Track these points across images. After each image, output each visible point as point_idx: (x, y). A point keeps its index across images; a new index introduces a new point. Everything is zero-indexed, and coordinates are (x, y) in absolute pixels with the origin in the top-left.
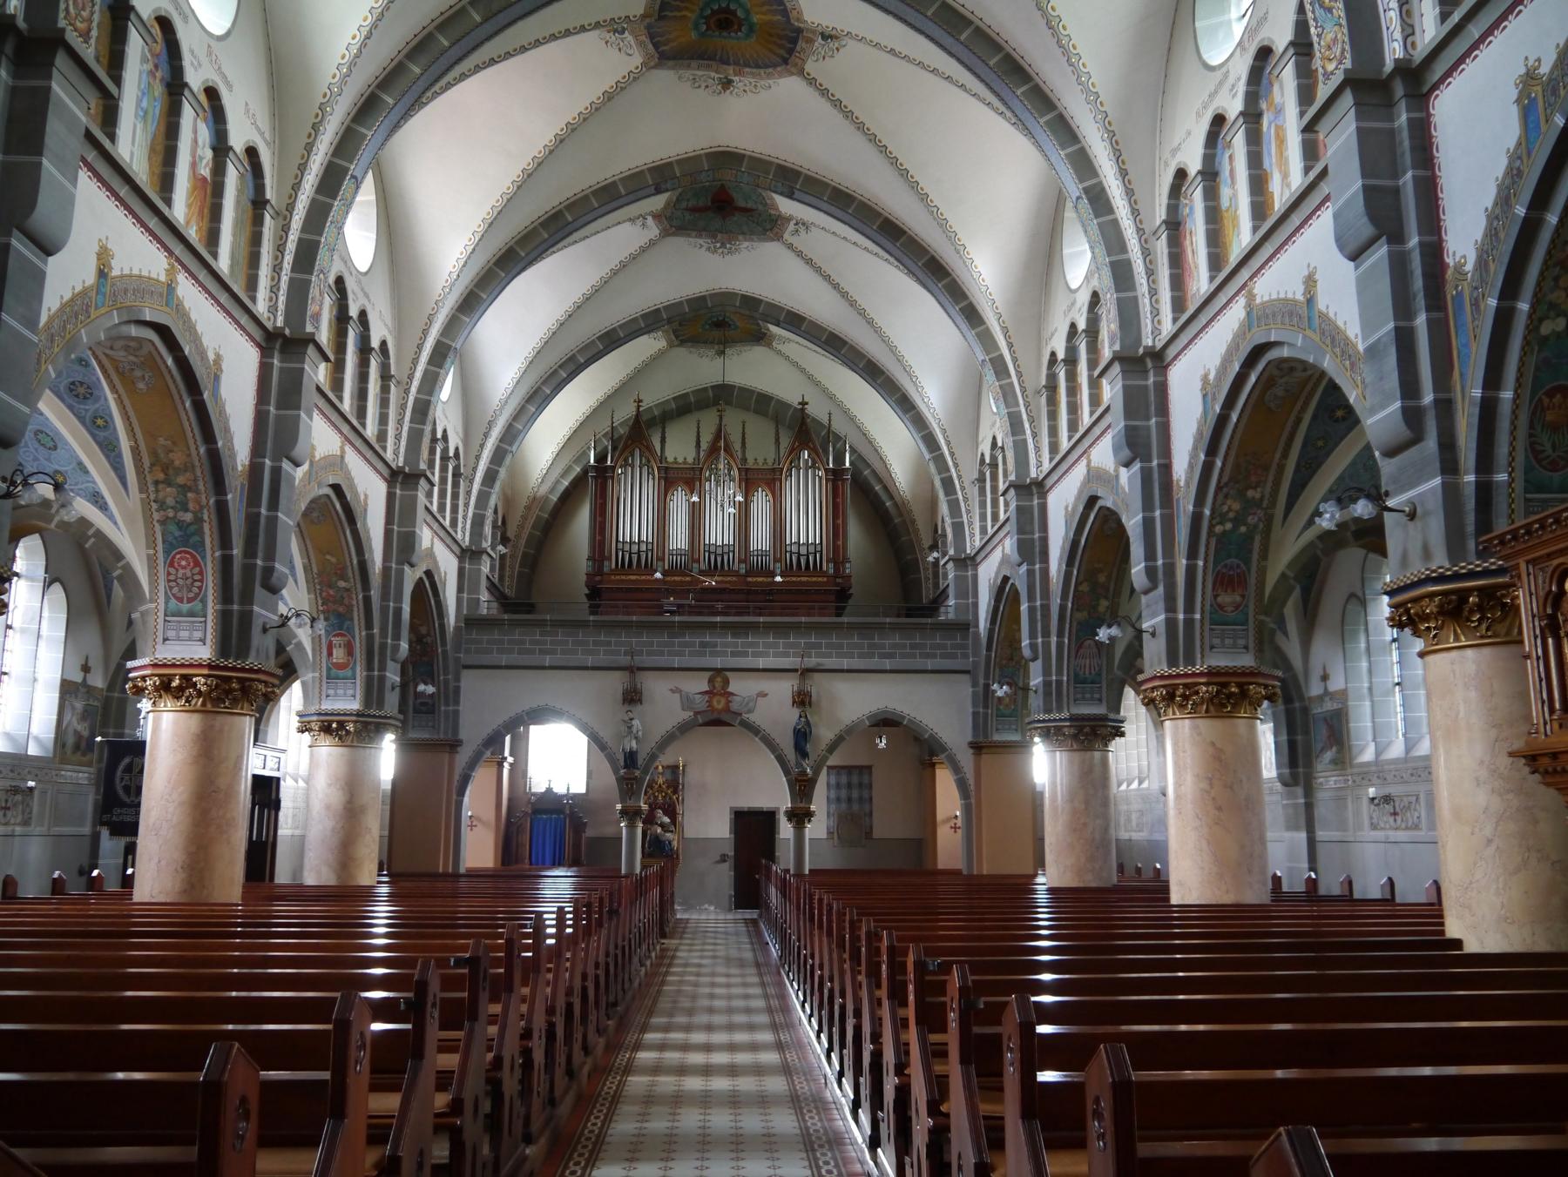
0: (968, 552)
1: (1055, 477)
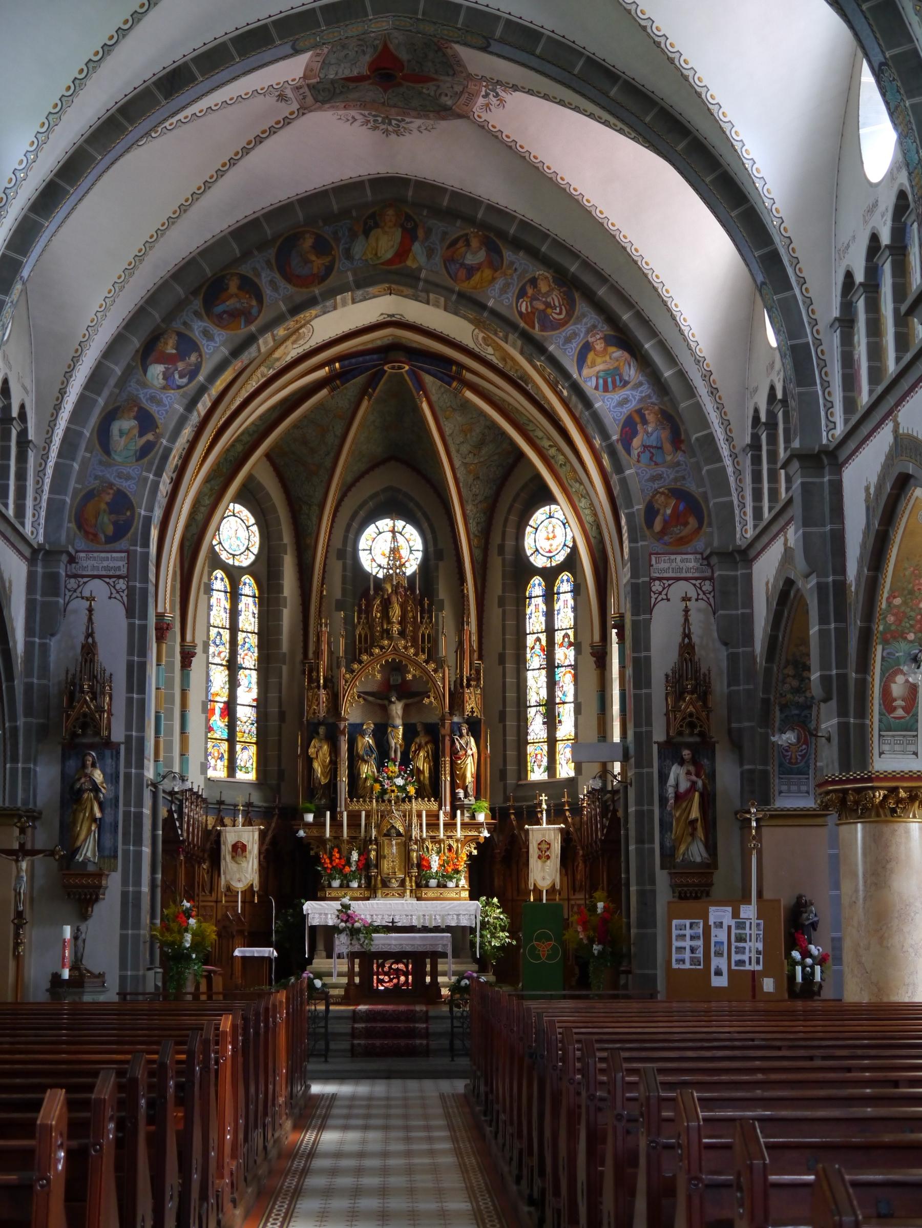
0: (738, 542)
1: (852, 445)
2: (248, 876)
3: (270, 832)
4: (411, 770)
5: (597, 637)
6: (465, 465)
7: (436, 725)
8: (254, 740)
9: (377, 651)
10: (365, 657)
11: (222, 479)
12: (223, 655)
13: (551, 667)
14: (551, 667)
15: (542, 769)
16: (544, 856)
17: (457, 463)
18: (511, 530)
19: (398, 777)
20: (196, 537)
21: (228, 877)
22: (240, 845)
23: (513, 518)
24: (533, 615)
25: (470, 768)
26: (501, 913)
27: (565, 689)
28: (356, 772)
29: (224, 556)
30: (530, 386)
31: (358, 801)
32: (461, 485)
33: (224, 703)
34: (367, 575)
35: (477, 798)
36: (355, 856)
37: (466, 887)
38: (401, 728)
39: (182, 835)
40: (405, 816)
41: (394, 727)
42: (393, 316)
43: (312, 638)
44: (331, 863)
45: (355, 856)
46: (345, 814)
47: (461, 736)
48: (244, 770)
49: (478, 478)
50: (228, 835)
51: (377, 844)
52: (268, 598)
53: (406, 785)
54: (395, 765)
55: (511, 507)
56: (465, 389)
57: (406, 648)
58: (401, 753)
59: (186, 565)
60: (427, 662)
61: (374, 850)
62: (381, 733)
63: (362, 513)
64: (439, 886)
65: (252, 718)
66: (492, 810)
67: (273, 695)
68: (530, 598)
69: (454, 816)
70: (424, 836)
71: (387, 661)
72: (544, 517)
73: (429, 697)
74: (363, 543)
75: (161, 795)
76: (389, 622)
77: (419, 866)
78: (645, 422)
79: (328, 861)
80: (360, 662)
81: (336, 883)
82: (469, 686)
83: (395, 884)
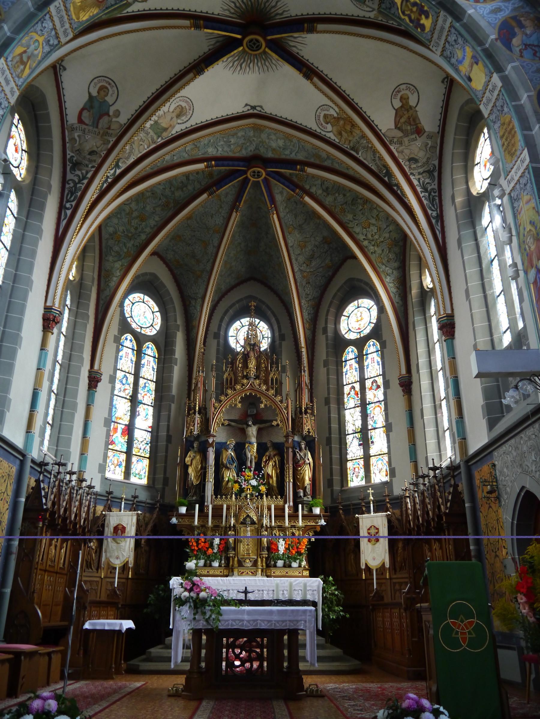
2: (125, 554)
3: (152, 521)
4: (263, 475)
5: (404, 371)
6: (301, 271)
8: (148, 456)
10: (229, 392)
11: (130, 258)
12: (127, 392)
13: (364, 405)
14: (364, 405)
15: (359, 479)
16: (374, 538)
17: (296, 269)
18: (331, 318)
20: (108, 298)
21: (108, 555)
22: (120, 527)
23: (333, 310)
24: (348, 372)
25: (307, 474)
26: (335, 590)
28: (221, 477)
29: (134, 326)
30: (360, 153)
31: (221, 498)
32: (298, 284)
33: (125, 425)
34: (232, 351)
35: (314, 496)
36: (217, 541)
37: (307, 567)
38: (255, 445)
39: (46, 504)
40: (258, 508)
41: (250, 443)
42: (254, 108)
44: (197, 546)
45: (217, 541)
47: (301, 450)
48: (138, 476)
49: (309, 283)
50: (111, 518)
51: (235, 530)
52: (164, 358)
53: (259, 485)
54: (251, 471)
55: (331, 302)
56: (304, 195)
57: (259, 385)
59: (100, 317)
62: (240, 448)
63: (231, 312)
64: (285, 566)
65: (147, 440)
67: (163, 424)
68: (346, 361)
69: (296, 510)
70: (273, 524)
71: (246, 395)
72: (354, 308)
74: (232, 332)
75: (29, 464)
77: (269, 549)
78: (521, 26)
79: (195, 544)
80: (227, 395)
82: (306, 413)
83: (248, 563)
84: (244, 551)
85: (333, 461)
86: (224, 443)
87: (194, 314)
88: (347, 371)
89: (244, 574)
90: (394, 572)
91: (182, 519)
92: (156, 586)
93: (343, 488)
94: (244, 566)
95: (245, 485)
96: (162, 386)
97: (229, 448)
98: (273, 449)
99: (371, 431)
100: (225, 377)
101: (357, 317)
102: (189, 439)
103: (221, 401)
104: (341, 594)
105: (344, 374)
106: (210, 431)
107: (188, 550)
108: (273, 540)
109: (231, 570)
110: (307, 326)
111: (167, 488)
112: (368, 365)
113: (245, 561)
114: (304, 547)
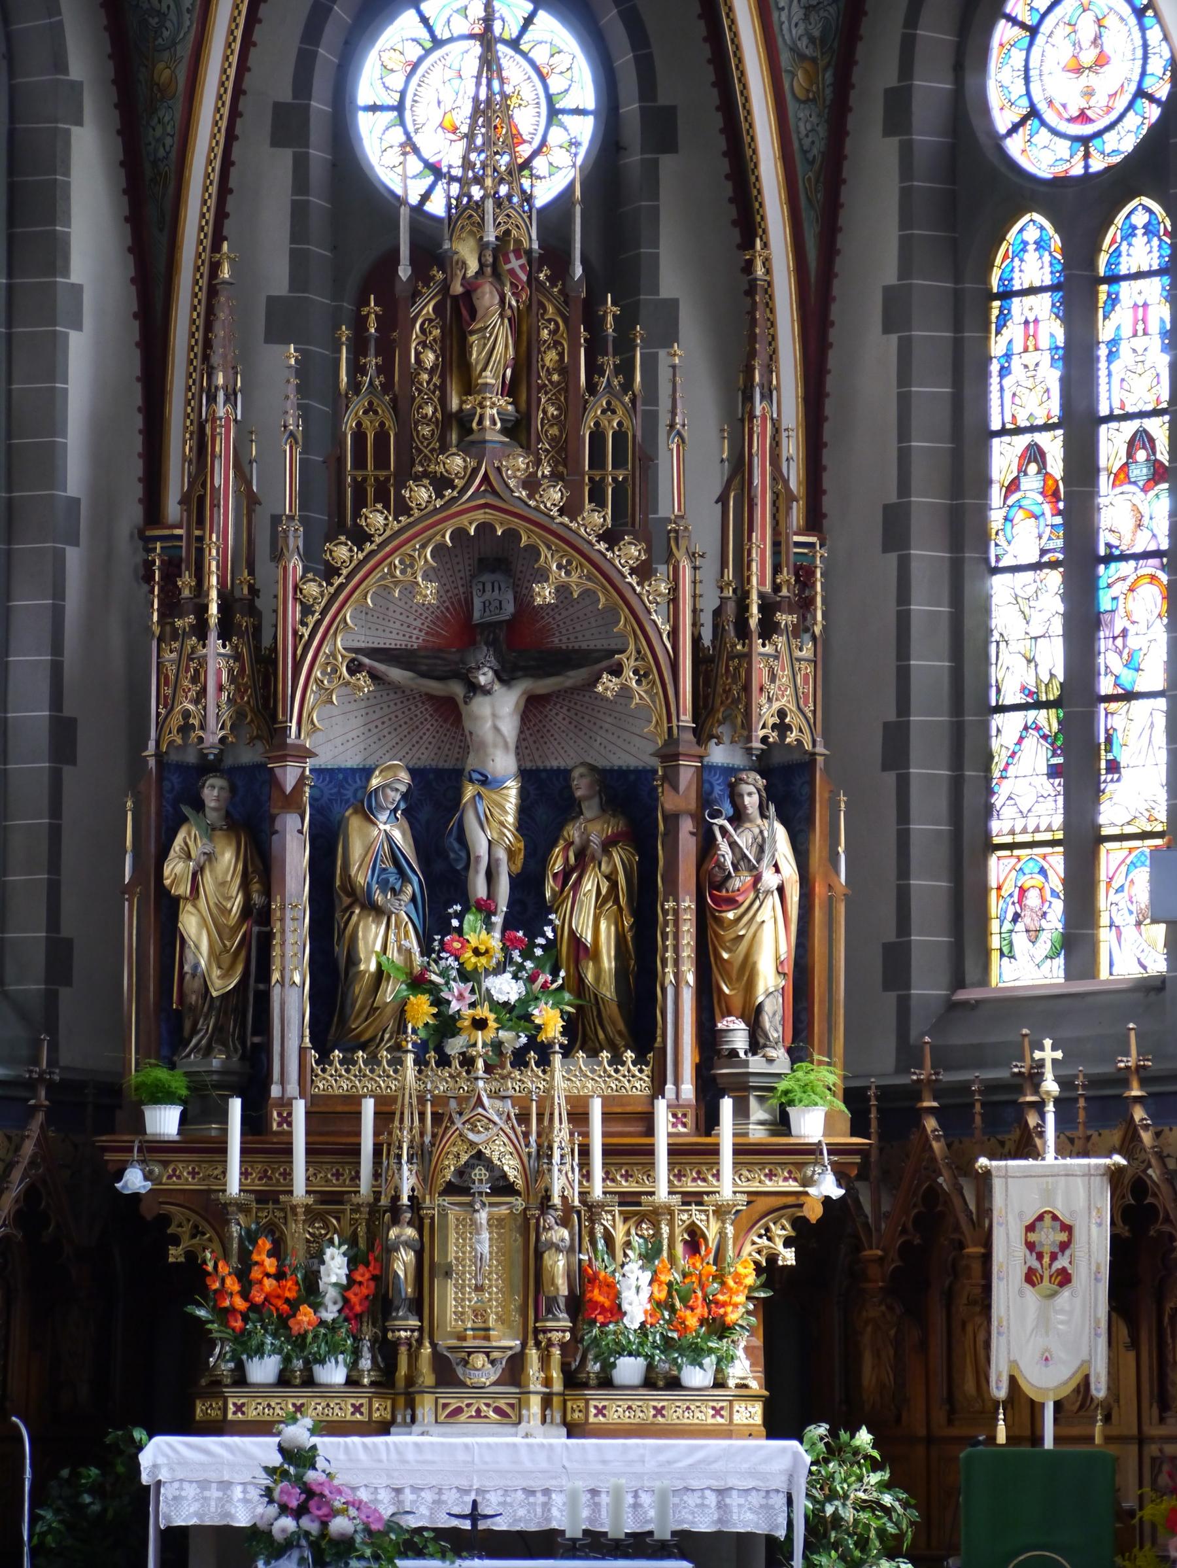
3: (16, 1174)
4: (550, 946)
7: (644, 775)
9: (422, 494)
10: (376, 519)
15: (1044, 945)
19: (499, 970)
24: (1016, 363)
26: (885, 1486)
27: (1133, 642)
28: (341, 952)
31: (347, 1062)
35: (797, 1055)
37: (754, 1385)
40: (523, 1118)
41: (485, 781)
43: (178, 446)
44: (245, 1295)
46: (300, 1109)
47: (739, 818)
54: (489, 927)
58: (514, 881)
60: (611, 537)
61: (408, 1244)
64: (649, 1382)
66: (853, 1097)
69: (709, 1120)
70: (598, 1190)
73: (617, 671)
76: (469, 387)
77: (577, 1305)
79: (232, 1284)
80: (360, 537)
81: (263, 1370)
82: (768, 629)
83: (484, 1372)
84: (460, 1316)
85: (915, 852)
86: (353, 771)
87: (162, 16)
88: (1008, 356)
89: (463, 1417)
90: (1155, 1411)
91: (165, 1164)
92: (65, 1473)
93: (961, 995)
94: (464, 1385)
95: (461, 997)
96: (9, 449)
97: (382, 808)
98: (603, 809)
99: (1113, 706)
100: (349, 424)
101: (1076, 44)
102: (174, 757)
103: (336, 572)
104: (905, 1505)
105: (995, 367)
106: (285, 730)
107: (202, 1313)
108: (597, 1265)
109: (401, 1400)
110: (797, 83)
111: (64, 992)
112: (1114, 342)
113: (466, 1363)
114: (741, 1298)
